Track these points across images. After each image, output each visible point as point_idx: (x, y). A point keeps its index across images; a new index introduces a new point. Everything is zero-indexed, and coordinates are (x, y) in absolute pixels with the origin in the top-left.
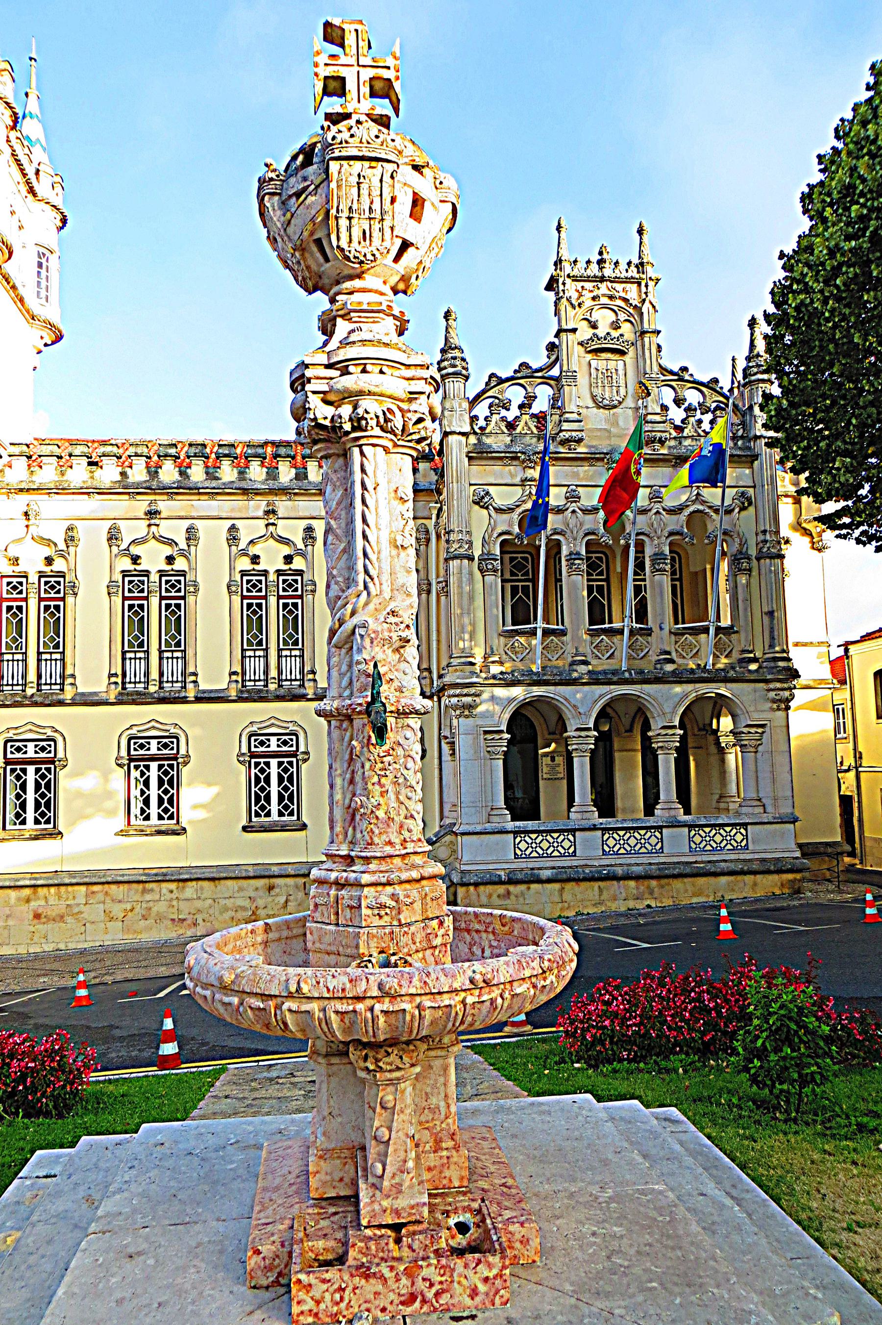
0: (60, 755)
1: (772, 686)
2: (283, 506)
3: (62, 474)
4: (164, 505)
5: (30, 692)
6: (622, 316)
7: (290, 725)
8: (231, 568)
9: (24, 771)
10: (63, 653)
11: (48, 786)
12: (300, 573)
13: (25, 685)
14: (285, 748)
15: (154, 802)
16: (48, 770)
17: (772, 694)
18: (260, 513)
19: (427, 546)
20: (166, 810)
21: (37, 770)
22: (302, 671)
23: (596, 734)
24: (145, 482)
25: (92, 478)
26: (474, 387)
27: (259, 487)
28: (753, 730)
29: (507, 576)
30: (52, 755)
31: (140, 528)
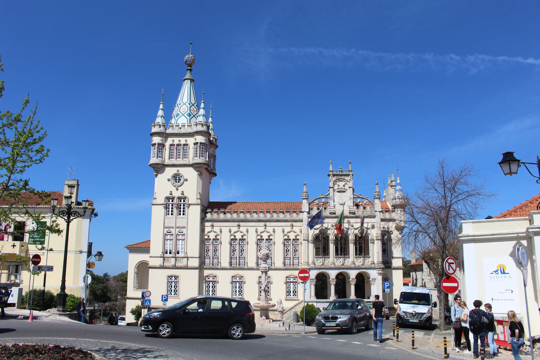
0: (217, 280)
1: (377, 270)
2: (268, 224)
3: (219, 216)
4: (241, 224)
6: (345, 183)
8: (257, 238)
9: (210, 283)
11: (215, 287)
12: (272, 239)
13: (210, 264)
15: (237, 291)
16: (215, 283)
17: (378, 271)
18: (263, 225)
19: (301, 233)
20: (240, 294)
21: (212, 283)
22: (271, 263)
23: (336, 280)
25: (225, 217)
27: (262, 219)
28: (373, 280)
31: (236, 229)
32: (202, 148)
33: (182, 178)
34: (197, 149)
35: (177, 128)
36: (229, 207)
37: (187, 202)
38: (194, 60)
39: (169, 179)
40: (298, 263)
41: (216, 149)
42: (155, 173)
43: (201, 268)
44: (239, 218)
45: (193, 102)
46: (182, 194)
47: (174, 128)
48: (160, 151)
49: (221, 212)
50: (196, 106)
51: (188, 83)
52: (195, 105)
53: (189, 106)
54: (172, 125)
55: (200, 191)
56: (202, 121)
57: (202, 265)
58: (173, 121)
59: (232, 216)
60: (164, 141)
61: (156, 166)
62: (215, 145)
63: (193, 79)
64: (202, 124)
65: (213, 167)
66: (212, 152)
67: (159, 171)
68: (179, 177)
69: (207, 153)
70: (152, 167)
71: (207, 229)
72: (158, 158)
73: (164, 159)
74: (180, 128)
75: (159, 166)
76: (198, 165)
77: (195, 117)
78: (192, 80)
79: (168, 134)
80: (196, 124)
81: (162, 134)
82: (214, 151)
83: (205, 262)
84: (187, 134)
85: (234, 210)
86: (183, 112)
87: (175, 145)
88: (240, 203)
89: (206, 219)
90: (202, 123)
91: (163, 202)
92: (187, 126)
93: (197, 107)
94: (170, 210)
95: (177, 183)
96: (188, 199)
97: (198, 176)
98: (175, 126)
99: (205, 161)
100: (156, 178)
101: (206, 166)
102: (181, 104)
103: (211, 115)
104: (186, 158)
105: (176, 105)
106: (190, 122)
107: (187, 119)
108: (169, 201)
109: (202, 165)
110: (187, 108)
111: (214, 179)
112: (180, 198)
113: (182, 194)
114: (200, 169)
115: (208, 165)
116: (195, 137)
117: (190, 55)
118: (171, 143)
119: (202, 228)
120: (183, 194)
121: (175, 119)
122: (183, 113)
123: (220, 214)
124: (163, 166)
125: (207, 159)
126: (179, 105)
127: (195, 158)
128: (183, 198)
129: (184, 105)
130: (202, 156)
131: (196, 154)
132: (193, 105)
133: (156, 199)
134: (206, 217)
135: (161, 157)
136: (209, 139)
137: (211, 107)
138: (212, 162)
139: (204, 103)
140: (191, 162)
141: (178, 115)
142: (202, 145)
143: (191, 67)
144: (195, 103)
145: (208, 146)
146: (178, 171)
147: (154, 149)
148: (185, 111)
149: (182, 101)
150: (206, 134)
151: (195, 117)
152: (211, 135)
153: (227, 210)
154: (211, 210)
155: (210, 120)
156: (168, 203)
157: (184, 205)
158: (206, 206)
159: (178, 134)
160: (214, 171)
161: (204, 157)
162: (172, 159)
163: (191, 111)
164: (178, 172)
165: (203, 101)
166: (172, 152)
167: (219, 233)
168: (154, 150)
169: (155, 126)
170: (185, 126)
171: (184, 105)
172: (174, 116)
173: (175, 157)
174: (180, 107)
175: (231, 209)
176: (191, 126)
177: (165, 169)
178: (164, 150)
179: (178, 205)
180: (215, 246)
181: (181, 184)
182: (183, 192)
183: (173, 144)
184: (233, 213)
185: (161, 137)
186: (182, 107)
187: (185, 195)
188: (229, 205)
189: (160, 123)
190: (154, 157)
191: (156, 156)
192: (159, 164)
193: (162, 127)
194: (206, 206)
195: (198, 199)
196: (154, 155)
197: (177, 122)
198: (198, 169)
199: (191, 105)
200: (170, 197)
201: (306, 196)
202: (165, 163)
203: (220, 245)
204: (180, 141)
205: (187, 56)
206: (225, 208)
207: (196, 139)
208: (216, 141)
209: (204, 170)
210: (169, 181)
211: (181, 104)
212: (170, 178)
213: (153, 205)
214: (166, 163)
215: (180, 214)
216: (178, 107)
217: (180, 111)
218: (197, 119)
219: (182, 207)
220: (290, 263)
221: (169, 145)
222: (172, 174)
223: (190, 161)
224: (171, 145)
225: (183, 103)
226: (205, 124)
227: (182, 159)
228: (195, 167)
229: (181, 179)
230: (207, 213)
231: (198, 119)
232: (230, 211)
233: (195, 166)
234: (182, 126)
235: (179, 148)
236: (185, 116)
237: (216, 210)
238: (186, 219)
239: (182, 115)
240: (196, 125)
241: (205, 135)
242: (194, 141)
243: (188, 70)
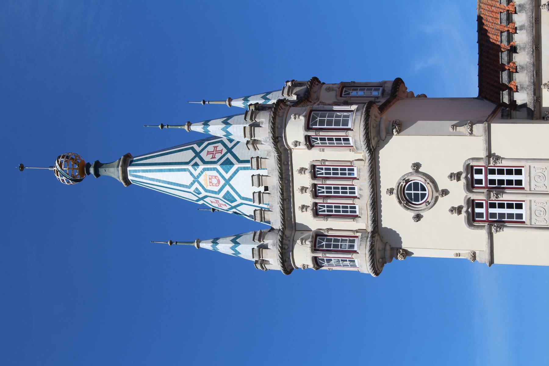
3: (522, 68)
24: (526, 13)
32: (322, 123)
33: (411, 178)
34: (324, 139)
35: (266, 197)
36: (494, 38)
37: (482, 163)
38: (67, 157)
39: (414, 218)
41: (324, 83)
42: (400, 258)
44: (527, 6)
45: (188, 155)
46: (459, 179)
47: (266, 206)
48: (336, 246)
49: (510, 60)
50: (199, 146)
51: (135, 171)
52: (198, 149)
53: (202, 167)
54: (258, 213)
55: (447, 124)
56: (242, 127)
58: (247, 210)
59: (522, 28)
60: (306, 234)
61: (378, 255)
62: (311, 87)
63: (122, 157)
64: (251, 126)
65: (375, 90)
66: (333, 93)
67: (393, 246)
68: (409, 188)
69: (336, 108)
70: (382, 266)
72: (355, 249)
73: (357, 231)
74: (266, 188)
75: (379, 245)
76: (372, 134)
77: (233, 147)
78: (128, 161)
79: (284, 224)
80: (253, 144)
81: (284, 241)
82: (329, 89)
84: (283, 168)
85: (504, 23)
86: (219, 182)
87: (317, 201)
88: (480, 7)
89: (530, 106)
90: (247, 126)
91: (483, 233)
92: (258, 168)
93: (203, 143)
94: (506, 211)
95: (427, 192)
96: (473, 159)
97: (400, 134)
98: (261, 205)
99: (359, 113)
100: (413, 254)
101: (375, 111)
102: (197, 189)
103: (223, 103)
104: (353, 170)
105: (201, 202)
106: (247, 161)
107: (240, 172)
108: (481, 215)
109: (372, 122)
111: (410, 86)
112: (471, 185)
113: (459, 179)
114: (383, 127)
115: (370, 105)
116: (292, 146)
117: (55, 169)
118: (309, 213)
120: (458, 176)
121: (242, 204)
122: (222, 182)
123: (517, 64)
124: (379, 235)
125: (354, 107)
126: (200, 196)
127: (352, 145)
128: (469, 176)
129: (201, 179)
130: (346, 123)
131: (340, 140)
132: (197, 154)
133: (474, 254)
134: (524, 106)
135: (350, 241)
136: (295, 104)
137: (202, 103)
138: (361, 93)
139: (189, 124)
140: (364, 154)
141: (229, 198)
142: (313, 125)
143: (88, 166)
144: (192, 149)
145: (315, 106)
146: (391, 191)
147: (329, 261)
148: (216, 177)
149: (189, 187)
150: (281, 114)
151: (233, 147)
152: (282, 98)
153: (505, 44)
154: (505, 93)
155: (238, 103)
156: (484, 219)
157: (492, 172)
158: (490, 107)
159: (282, 194)
160: (389, 87)
161: (348, 117)
162: (357, 210)
163: (215, 160)
164: (395, 191)
165: (184, 125)
166: (336, 211)
168: (332, 262)
169: (263, 260)
170: (259, 175)
171: (200, 180)
172: (235, 207)
173: (350, 201)
175: (502, 32)
176: (258, 158)
177: (386, 228)
178: (331, 233)
179: (490, 190)
181: (428, 181)
182: (451, 176)
183: (313, 209)
184: (511, 25)
185: (294, 242)
186: (205, 186)
187: (460, 168)
188: (489, 37)
189: (255, 246)
190: (354, 261)
191: (350, 256)
192: (372, 247)
193: (266, 242)
194: (493, 106)
195: (471, 130)
196: (348, 263)
197: (249, 200)
198: (383, 134)
199: (197, 160)
200: (467, 212)
202: (370, 229)
204: (303, 189)
205: (59, 177)
206: (497, 49)
207: (296, 143)
208: (300, 84)
209: (384, 116)
210: (422, 216)
211: (197, 189)
212: (412, 214)
213: (492, 262)
214: (367, 226)
215: (519, 182)
216: (206, 197)
217: (217, 190)
218: (238, 142)
219: (496, 177)
221: (317, 219)
222: (400, 208)
223: (360, 156)
224: (316, 214)
225: (192, 184)
226: (251, 119)
227: (355, 181)
228: (378, 143)
229: (414, 183)
230: (513, 102)
231: (237, 139)
232: (505, 34)
233: (373, 143)
234: (259, 186)
235: (325, 190)
236: (231, 178)
237: (505, 76)
238: (532, 164)
239: (227, 186)
240: (255, 143)
241: (283, 116)
242: (303, 146)
243: (97, 174)
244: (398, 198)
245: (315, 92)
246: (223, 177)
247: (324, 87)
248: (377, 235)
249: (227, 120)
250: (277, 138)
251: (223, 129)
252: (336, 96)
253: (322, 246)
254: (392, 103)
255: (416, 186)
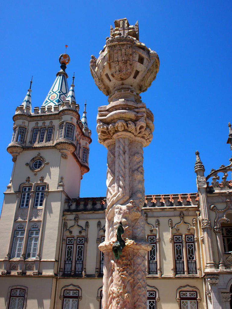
0: (80, 295)
5: (72, 274)
7: (153, 288)
10: (83, 261)
13: (71, 271)
14: (151, 296)
26: (207, 173)
29: (225, 234)
30: (77, 295)
39: (27, 163)
40: (196, 268)
43: (58, 278)
52: (66, 95)
57: (60, 273)
65: (85, 160)
67: (18, 157)
68: (40, 162)
71: (70, 223)
82: (86, 144)
83: (65, 269)
84: (53, 117)
110: (56, 95)
119: (63, 222)
122: (52, 100)
129: (54, 94)
132: (64, 94)
149: (52, 91)
160: (86, 164)
163: (61, 98)
167: (84, 228)
174: (50, 96)
178: (26, 133)
180: (79, 247)
199: (62, 93)
201: (199, 167)
203: (86, 244)
204: (44, 123)
217: (49, 99)
220: (184, 269)
233: (58, 147)
239: (50, 101)
244: (36, 157)
245: (85, 139)
246: (54, 100)
247: (88, 143)
248: (22, 149)
249: (74, 97)
250: (64, 112)
251: (70, 95)
252: (84, 146)
253: (21, 130)
254: (78, 163)
255: (40, 165)
